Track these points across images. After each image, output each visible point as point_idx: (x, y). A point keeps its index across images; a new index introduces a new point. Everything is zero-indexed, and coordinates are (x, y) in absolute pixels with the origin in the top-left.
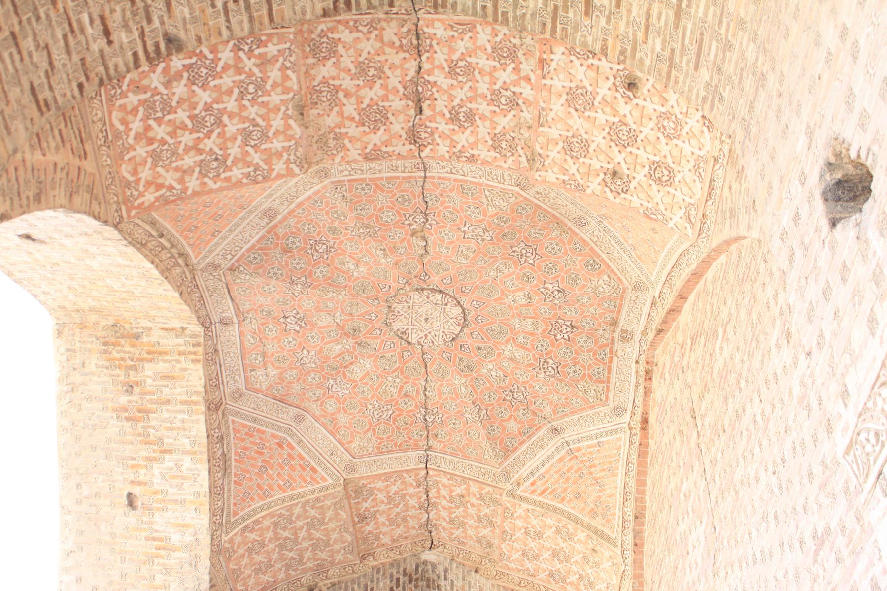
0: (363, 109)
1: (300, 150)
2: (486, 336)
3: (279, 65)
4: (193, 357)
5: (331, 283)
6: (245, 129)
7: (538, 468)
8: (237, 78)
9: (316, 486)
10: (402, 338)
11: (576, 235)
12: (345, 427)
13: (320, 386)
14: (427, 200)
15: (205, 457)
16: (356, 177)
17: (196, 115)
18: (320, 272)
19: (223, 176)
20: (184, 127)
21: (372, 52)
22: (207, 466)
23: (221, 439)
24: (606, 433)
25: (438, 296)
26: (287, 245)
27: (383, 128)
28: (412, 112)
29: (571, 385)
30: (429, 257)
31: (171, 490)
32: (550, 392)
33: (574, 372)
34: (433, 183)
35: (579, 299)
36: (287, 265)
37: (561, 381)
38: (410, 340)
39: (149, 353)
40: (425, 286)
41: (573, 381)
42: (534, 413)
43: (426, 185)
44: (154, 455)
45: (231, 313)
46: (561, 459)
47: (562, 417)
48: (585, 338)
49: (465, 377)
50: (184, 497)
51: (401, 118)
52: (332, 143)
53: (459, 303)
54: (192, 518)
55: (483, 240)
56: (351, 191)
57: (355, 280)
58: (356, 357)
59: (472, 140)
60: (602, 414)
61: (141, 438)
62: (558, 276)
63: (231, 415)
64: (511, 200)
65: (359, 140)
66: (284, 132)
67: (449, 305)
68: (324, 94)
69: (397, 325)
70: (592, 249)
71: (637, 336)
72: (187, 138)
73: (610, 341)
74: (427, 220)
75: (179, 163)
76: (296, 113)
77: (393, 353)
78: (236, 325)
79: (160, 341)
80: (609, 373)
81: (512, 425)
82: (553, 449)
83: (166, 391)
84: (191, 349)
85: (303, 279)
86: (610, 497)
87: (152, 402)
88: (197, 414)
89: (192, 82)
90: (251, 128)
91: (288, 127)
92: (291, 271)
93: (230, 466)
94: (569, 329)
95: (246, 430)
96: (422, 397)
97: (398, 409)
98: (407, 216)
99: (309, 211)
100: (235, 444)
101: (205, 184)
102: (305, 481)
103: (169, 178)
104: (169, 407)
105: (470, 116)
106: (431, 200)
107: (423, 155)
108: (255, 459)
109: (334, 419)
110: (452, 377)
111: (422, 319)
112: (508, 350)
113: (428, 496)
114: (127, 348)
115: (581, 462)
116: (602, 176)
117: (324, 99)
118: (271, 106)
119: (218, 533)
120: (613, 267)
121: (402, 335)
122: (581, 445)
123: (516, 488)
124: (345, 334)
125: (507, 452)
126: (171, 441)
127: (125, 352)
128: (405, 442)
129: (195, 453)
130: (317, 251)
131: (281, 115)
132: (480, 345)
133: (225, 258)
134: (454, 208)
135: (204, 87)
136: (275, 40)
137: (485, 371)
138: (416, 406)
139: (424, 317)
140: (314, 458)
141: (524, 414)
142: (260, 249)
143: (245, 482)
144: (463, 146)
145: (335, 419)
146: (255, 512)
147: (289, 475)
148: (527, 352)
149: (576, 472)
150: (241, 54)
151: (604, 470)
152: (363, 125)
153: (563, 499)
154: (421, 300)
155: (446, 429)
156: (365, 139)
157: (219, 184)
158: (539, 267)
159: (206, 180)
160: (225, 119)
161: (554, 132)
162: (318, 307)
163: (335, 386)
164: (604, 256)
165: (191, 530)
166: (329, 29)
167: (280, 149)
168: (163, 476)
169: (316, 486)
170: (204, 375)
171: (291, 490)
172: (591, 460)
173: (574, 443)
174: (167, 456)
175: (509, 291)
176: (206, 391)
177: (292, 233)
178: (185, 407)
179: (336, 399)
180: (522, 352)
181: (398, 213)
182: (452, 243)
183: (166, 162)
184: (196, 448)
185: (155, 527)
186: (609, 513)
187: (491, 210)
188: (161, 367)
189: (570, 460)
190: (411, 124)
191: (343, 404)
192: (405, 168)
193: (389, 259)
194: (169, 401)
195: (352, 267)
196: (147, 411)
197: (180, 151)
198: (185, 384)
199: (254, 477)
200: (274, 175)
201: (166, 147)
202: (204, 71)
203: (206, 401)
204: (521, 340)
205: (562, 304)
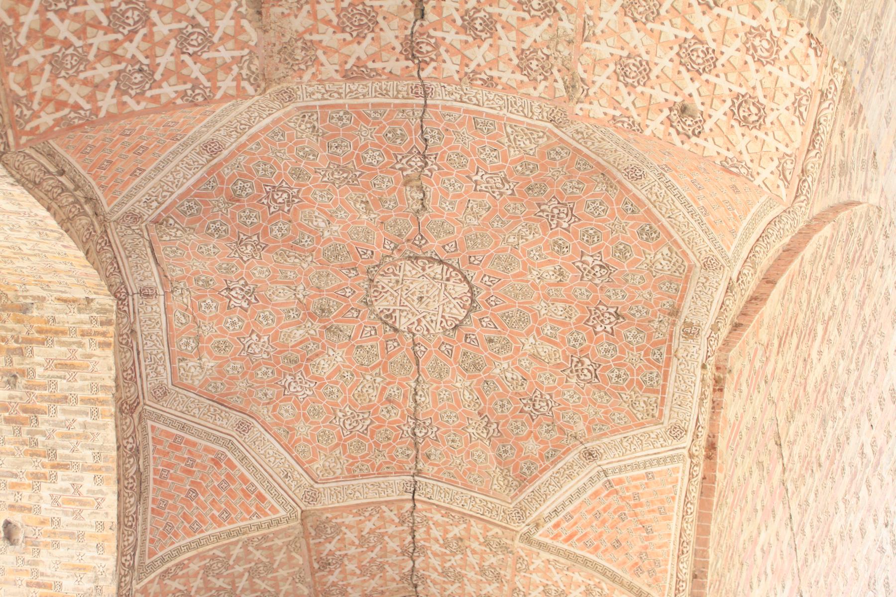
0: (343, 9)
1: (256, 62)
2: (501, 325)
4: (101, 339)
5: (293, 245)
6: (180, 30)
7: (563, 505)
9: (263, 519)
10: (386, 323)
11: (628, 191)
12: (305, 440)
13: (274, 383)
14: (428, 136)
15: (114, 475)
16: (331, 102)
17: (114, 8)
19: (149, 94)
20: (97, 25)
22: (115, 488)
23: (136, 452)
24: (658, 461)
25: (438, 268)
26: (235, 191)
27: (370, 36)
28: (411, 16)
30: (426, 215)
31: (64, 519)
32: (585, 403)
33: (618, 376)
34: (436, 114)
35: (629, 278)
36: (233, 219)
37: (600, 388)
38: (397, 325)
39: (40, 331)
40: (420, 254)
41: (615, 388)
42: (561, 429)
43: (427, 116)
44: (43, 470)
45: (155, 281)
46: (596, 494)
48: (634, 332)
49: (469, 378)
50: (81, 529)
51: (395, 23)
52: (299, 54)
53: (465, 278)
54: (93, 558)
55: (501, 194)
56: (324, 121)
57: (325, 243)
58: (324, 346)
59: (490, 56)
61: (26, 447)
62: (600, 247)
63: (151, 419)
64: (541, 141)
65: (337, 51)
66: (235, 37)
67: (452, 280)
69: (379, 306)
70: (648, 211)
71: (706, 331)
72: (100, 40)
73: (667, 336)
74: (426, 164)
75: (89, 74)
76: (251, 11)
77: (374, 343)
78: (162, 298)
79: (57, 316)
80: (665, 380)
81: (532, 447)
82: (585, 480)
83: (62, 383)
84: (100, 328)
85: (255, 238)
86: (660, 547)
87: (42, 398)
88: (104, 416)
90: (190, 29)
91: (240, 30)
92: (238, 226)
93: (147, 488)
94: (613, 319)
96: (410, 403)
97: (378, 419)
98: (400, 157)
99: (267, 147)
100: (154, 458)
101: (125, 103)
102: (248, 512)
103: (75, 94)
104: (66, 407)
105: (490, 24)
106: (432, 137)
107: (423, 74)
108: (181, 480)
109: (290, 430)
110: (453, 377)
111: (415, 298)
112: (529, 344)
113: (414, 537)
114: (10, 324)
115: (623, 499)
116: (666, 112)
119: (128, 578)
120: (676, 236)
121: (387, 319)
122: (623, 475)
123: (533, 530)
124: (310, 314)
125: (523, 481)
126: (67, 452)
127: (7, 330)
128: (386, 463)
129: (100, 469)
130: (275, 201)
131: (230, 12)
132: (492, 336)
133: (149, 207)
134: (462, 149)
137: (497, 371)
138: (403, 416)
139: (418, 295)
141: (548, 431)
142: (196, 195)
143: (167, 511)
144: (479, 65)
145: (292, 429)
146: (179, 551)
148: (555, 348)
149: (615, 512)
151: (653, 511)
153: (597, 548)
154: (414, 272)
155: (443, 448)
156: (345, 50)
157: (143, 105)
158: (575, 233)
159: (126, 98)
160: (154, 15)
161: (603, 50)
162: (274, 277)
163: (293, 384)
164: (665, 221)
165: (90, 574)
167: (228, 60)
168: (55, 500)
169: (263, 519)
170: (116, 363)
171: (229, 523)
172: (636, 496)
173: (614, 473)
174: (60, 473)
175: (532, 263)
176: (117, 386)
177: (240, 175)
178: (87, 407)
179: (294, 402)
180: (548, 347)
181: (387, 152)
182: (460, 196)
183: (71, 72)
184: (101, 464)
185: (41, 569)
186: (657, 569)
187: (514, 154)
188: (57, 351)
189: (608, 496)
190: (408, 32)
191: (304, 409)
192: (398, 92)
193: (373, 216)
194: (66, 398)
195: (322, 225)
196: (36, 412)
197: (91, 57)
198: (88, 375)
199: (179, 505)
200: (219, 95)
201: (70, 51)
203: (117, 400)
204: (548, 330)
205: (605, 285)
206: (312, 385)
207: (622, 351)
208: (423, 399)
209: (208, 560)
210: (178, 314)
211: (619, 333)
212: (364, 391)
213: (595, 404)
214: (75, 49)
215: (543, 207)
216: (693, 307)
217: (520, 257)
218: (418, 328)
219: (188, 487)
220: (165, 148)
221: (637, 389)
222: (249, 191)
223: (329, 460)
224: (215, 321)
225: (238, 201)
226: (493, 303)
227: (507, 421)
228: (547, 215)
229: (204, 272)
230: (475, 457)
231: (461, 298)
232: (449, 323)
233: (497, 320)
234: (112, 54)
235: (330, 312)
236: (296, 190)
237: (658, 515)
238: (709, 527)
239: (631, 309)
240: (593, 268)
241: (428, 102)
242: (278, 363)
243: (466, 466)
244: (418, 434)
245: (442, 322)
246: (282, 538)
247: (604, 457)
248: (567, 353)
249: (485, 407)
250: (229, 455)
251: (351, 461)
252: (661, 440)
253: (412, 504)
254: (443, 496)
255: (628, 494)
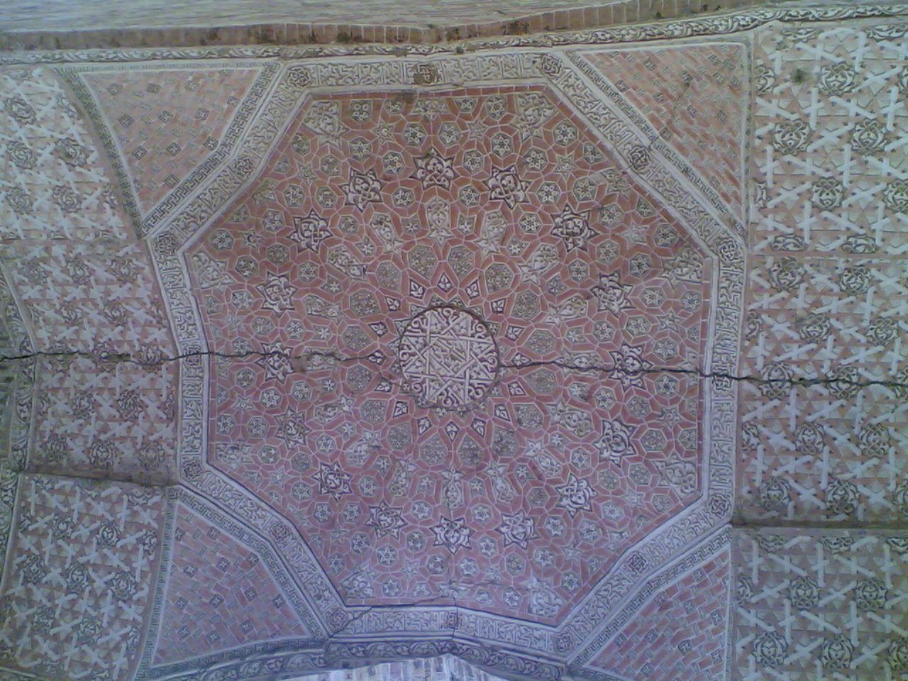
0: (121, 416)
3: (48, 495)
5: (384, 478)
8: (50, 537)
11: (265, 173)
14: (243, 352)
16: (204, 433)
18: (367, 487)
19: (138, 579)
20: (73, 602)
21: (66, 400)
29: (525, 147)
33: (502, 145)
34: (218, 345)
36: (351, 527)
37: (522, 164)
41: (517, 146)
45: (439, 614)
46: (681, 148)
47: (608, 153)
49: (545, 308)
51: (134, 377)
52: (151, 454)
56: (226, 439)
57: (385, 445)
58: (523, 460)
60: (571, 92)
62: (333, 187)
63: (585, 662)
66: (114, 503)
67: (423, 326)
68: (99, 454)
72: (84, 605)
73: (443, 98)
75: (105, 620)
76: (97, 489)
80: (492, 90)
81: (633, 234)
85: (373, 511)
89: (37, 582)
90: (99, 536)
92: (358, 524)
94: (434, 161)
95: (616, 649)
96: (590, 374)
97: (613, 412)
98: (269, 376)
99: (272, 488)
102: (719, 588)
103: (115, 634)
105: (114, 305)
108: (663, 654)
110: (548, 327)
111: (454, 363)
112: (487, 247)
113: (815, 381)
117: (105, 454)
118: (84, 511)
125: (683, 241)
130: (337, 487)
131: (93, 503)
135: (46, 571)
136: (27, 493)
137: (534, 278)
140: (692, 560)
142: (326, 555)
147: (707, 609)
150: (31, 528)
151: (659, 75)
152: (137, 418)
159: (135, 598)
160: (82, 560)
163: (574, 499)
166: (41, 440)
167: (129, 512)
177: (309, 513)
180: (486, 224)
181: (264, 386)
183: (98, 631)
189: (678, 133)
193: (343, 401)
195: (365, 447)
199: (689, 666)
200: (155, 525)
201: (82, 627)
202: (34, 566)
204: (466, 228)
206: (574, 479)
207: (470, 145)
208: (584, 360)
209: (751, 658)
210: (478, 599)
211: (449, 152)
212: (574, 424)
213: (550, 166)
214: (83, 623)
215: (303, 245)
216: (386, 81)
217: (376, 263)
218: (491, 361)
219: (675, 649)
220: (261, 572)
221: (512, 121)
222: (325, 508)
223: (669, 476)
224: (484, 564)
225: (334, 520)
226: (448, 285)
227: (599, 266)
228: (315, 241)
229: (422, 563)
230: (655, 301)
231: (447, 318)
232: (479, 330)
233: (467, 280)
234: (98, 598)
235: (477, 449)
236: (323, 467)
237: (659, 69)
238: (600, 8)
239: (413, 144)
240: (359, 192)
241: (206, 351)
242: (541, 511)
243: (670, 312)
244: (637, 365)
245: (480, 337)
246: (750, 556)
247: (637, 142)
248: (487, 205)
249: (580, 292)
250: (662, 589)
251: (674, 450)
252: (571, 81)
253: (745, 383)
254: (728, 342)
255: (665, 110)
